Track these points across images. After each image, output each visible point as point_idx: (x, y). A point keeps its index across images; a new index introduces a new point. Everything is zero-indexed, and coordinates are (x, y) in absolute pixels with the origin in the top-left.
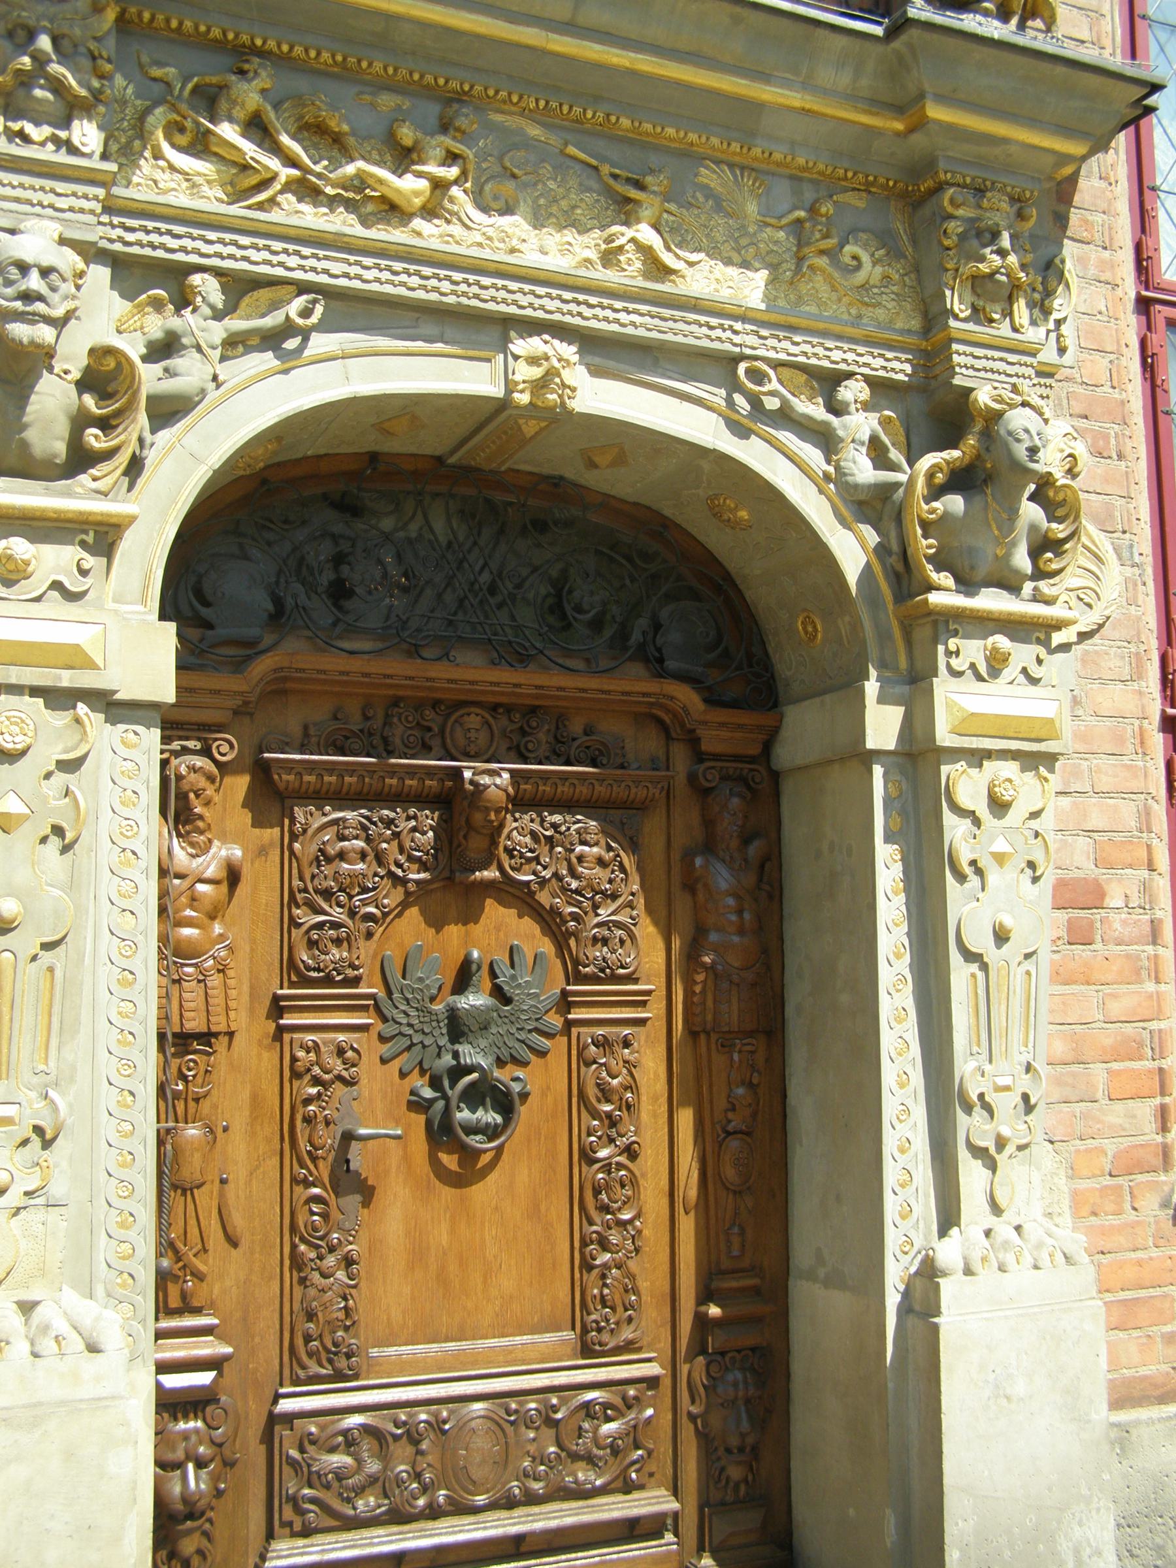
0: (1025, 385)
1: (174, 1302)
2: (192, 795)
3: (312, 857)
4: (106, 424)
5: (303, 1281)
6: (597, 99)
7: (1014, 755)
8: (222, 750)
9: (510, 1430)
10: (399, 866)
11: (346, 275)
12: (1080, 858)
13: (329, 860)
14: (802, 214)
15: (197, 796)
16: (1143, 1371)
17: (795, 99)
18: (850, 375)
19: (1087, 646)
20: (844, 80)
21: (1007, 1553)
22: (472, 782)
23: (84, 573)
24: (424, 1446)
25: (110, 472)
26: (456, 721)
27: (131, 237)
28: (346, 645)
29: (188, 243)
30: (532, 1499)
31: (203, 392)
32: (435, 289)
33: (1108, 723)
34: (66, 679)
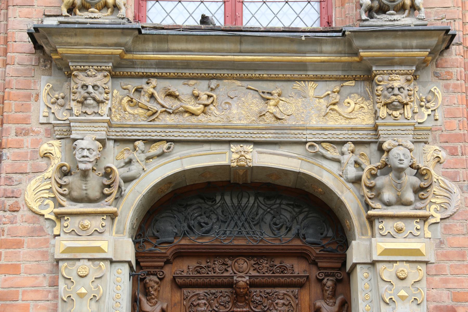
0: (400, 140)
2: (150, 288)
3: (189, 305)
4: (109, 186)
7: (407, 262)
8: (160, 274)
10: (217, 307)
11: (179, 136)
13: (195, 306)
14: (329, 92)
15: (152, 288)
19: (447, 222)
22: (236, 280)
23: (103, 227)
25: (111, 199)
26: (235, 262)
27: (118, 134)
29: (134, 133)
31: (140, 174)
32: (206, 136)
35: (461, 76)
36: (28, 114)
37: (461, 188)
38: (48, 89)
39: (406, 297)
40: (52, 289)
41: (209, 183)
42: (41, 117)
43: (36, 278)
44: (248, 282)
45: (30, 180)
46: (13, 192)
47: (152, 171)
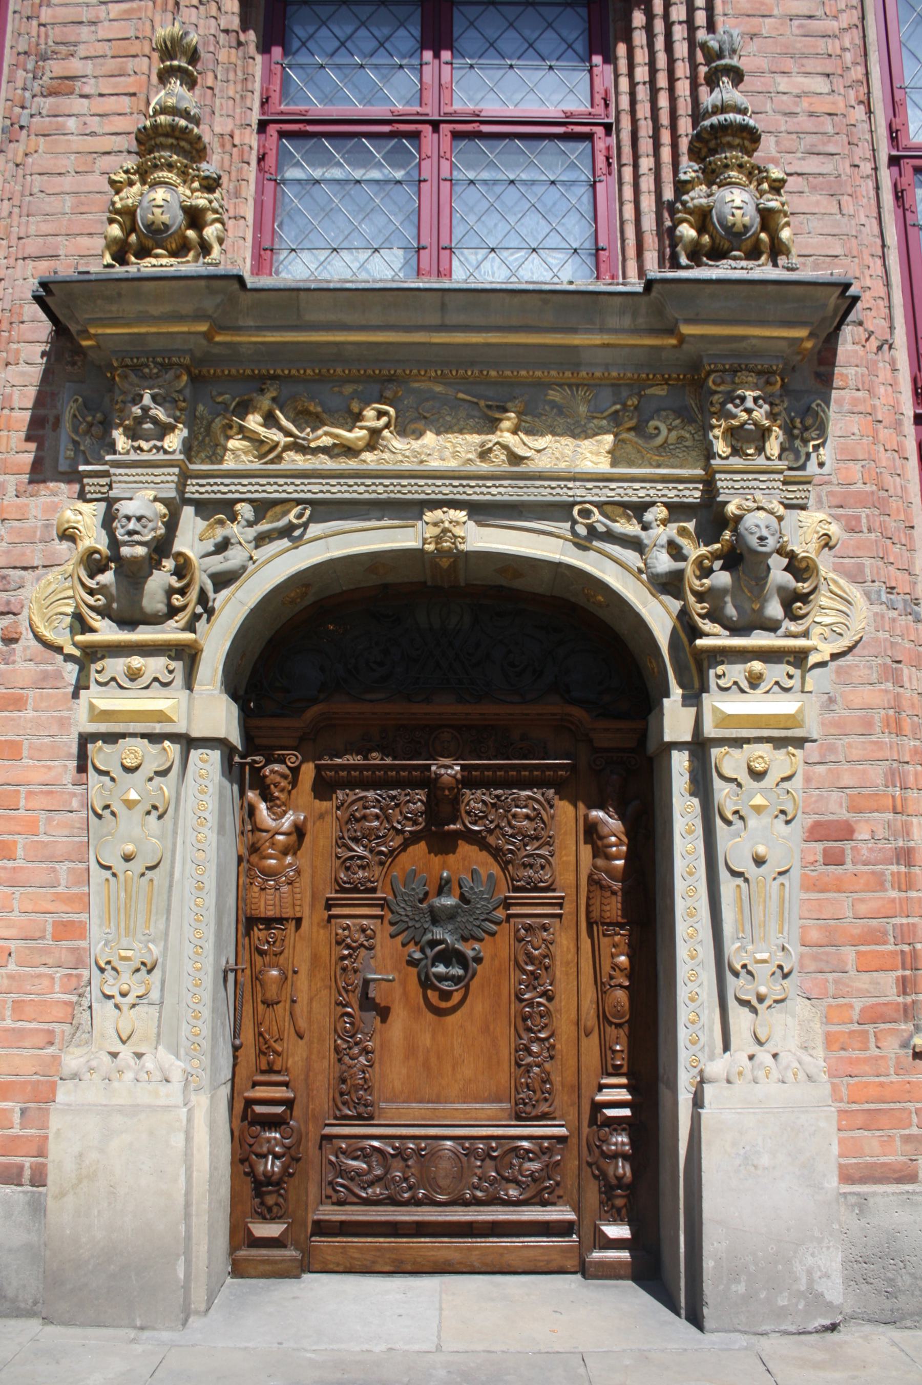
0: (758, 495)
4: (182, 592)
5: (340, 1060)
6: (472, 364)
7: (768, 740)
9: (464, 1159)
10: (399, 823)
11: (321, 492)
12: (836, 808)
13: (358, 820)
14: (618, 407)
16: (883, 1159)
17: (597, 339)
18: (653, 504)
19: (841, 662)
20: (627, 322)
21: (752, 1268)
22: (435, 773)
23: (171, 672)
24: (410, 1163)
25: (182, 618)
27: (202, 490)
28: (368, 697)
29: (233, 488)
30: (478, 1202)
31: (244, 568)
32: (374, 492)
33: (859, 713)
34: (158, 728)
37: (867, 594)
38: (75, 406)
39: (765, 807)
40: (79, 790)
41: (386, 586)
42: (61, 460)
44: (459, 776)
47: (268, 561)
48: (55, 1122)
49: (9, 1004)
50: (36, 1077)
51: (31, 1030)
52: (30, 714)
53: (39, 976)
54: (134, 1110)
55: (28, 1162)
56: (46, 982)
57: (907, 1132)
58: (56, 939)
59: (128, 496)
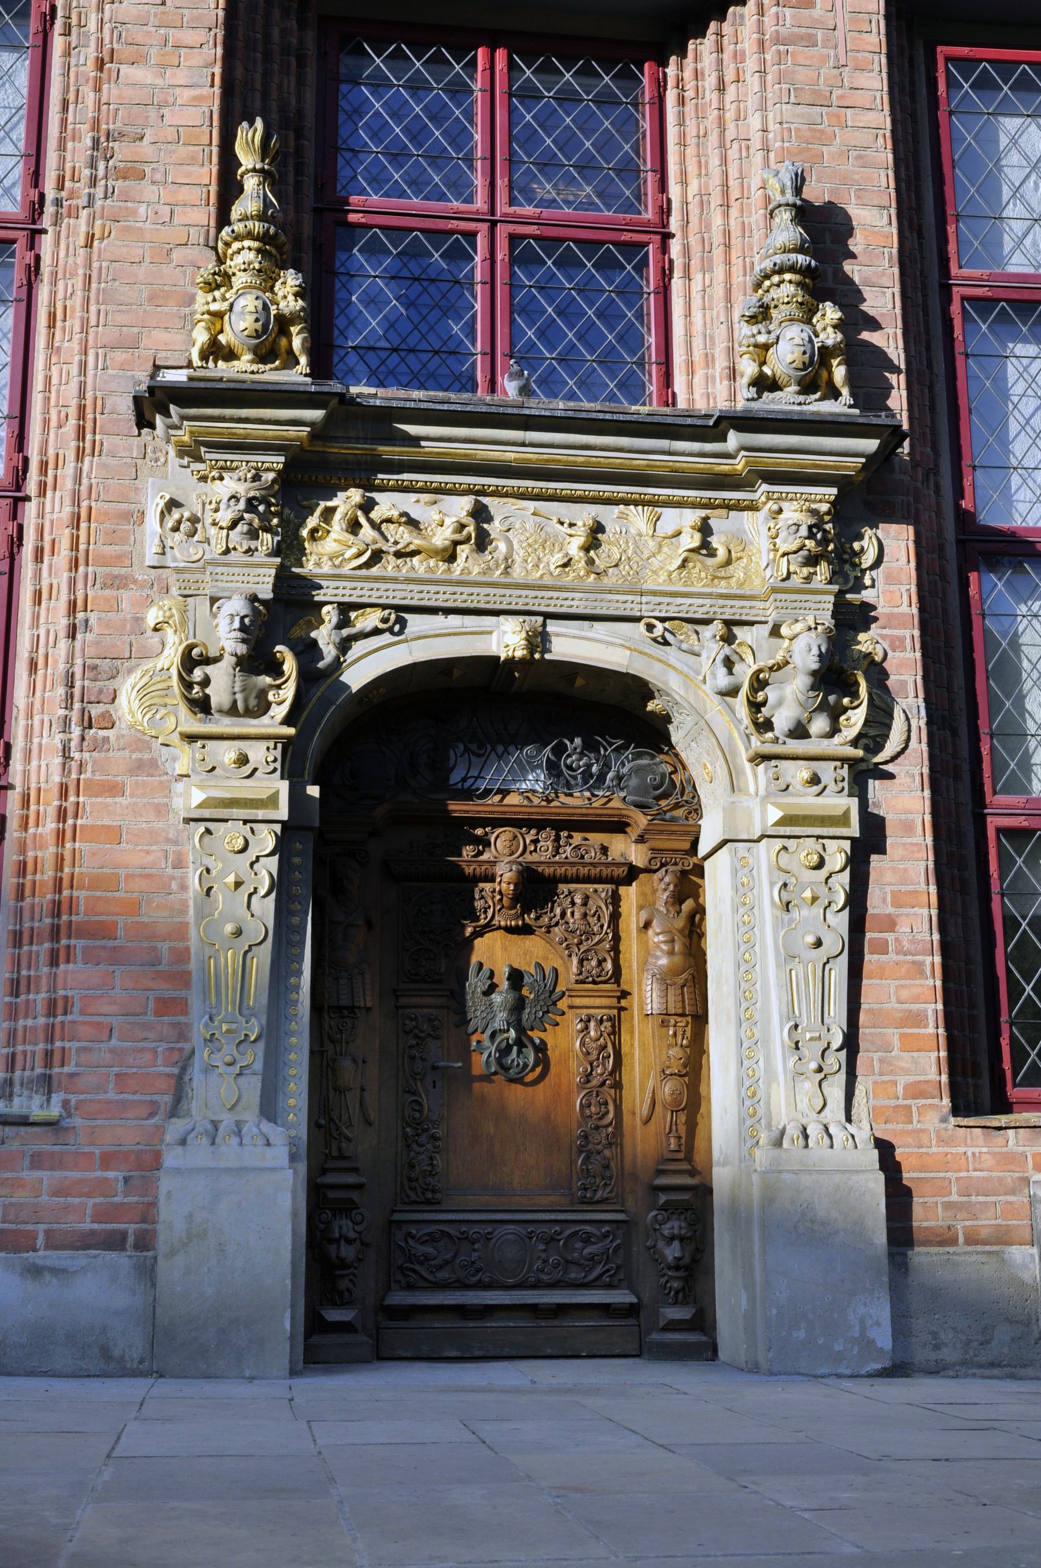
1: (335, 1153)
5: (408, 1146)
21: (811, 1316)
24: (476, 1246)
34: (261, 814)
35: (909, 511)
36: (126, 548)
43: (148, 852)
45: (130, 671)
46: (101, 691)
48: (166, 1184)
49: (112, 1078)
50: (140, 1147)
51: (133, 1101)
52: (124, 801)
53: (142, 1050)
54: (240, 1171)
55: (132, 1228)
56: (148, 1056)
57: (946, 1199)
58: (158, 1013)
59: (226, 594)
